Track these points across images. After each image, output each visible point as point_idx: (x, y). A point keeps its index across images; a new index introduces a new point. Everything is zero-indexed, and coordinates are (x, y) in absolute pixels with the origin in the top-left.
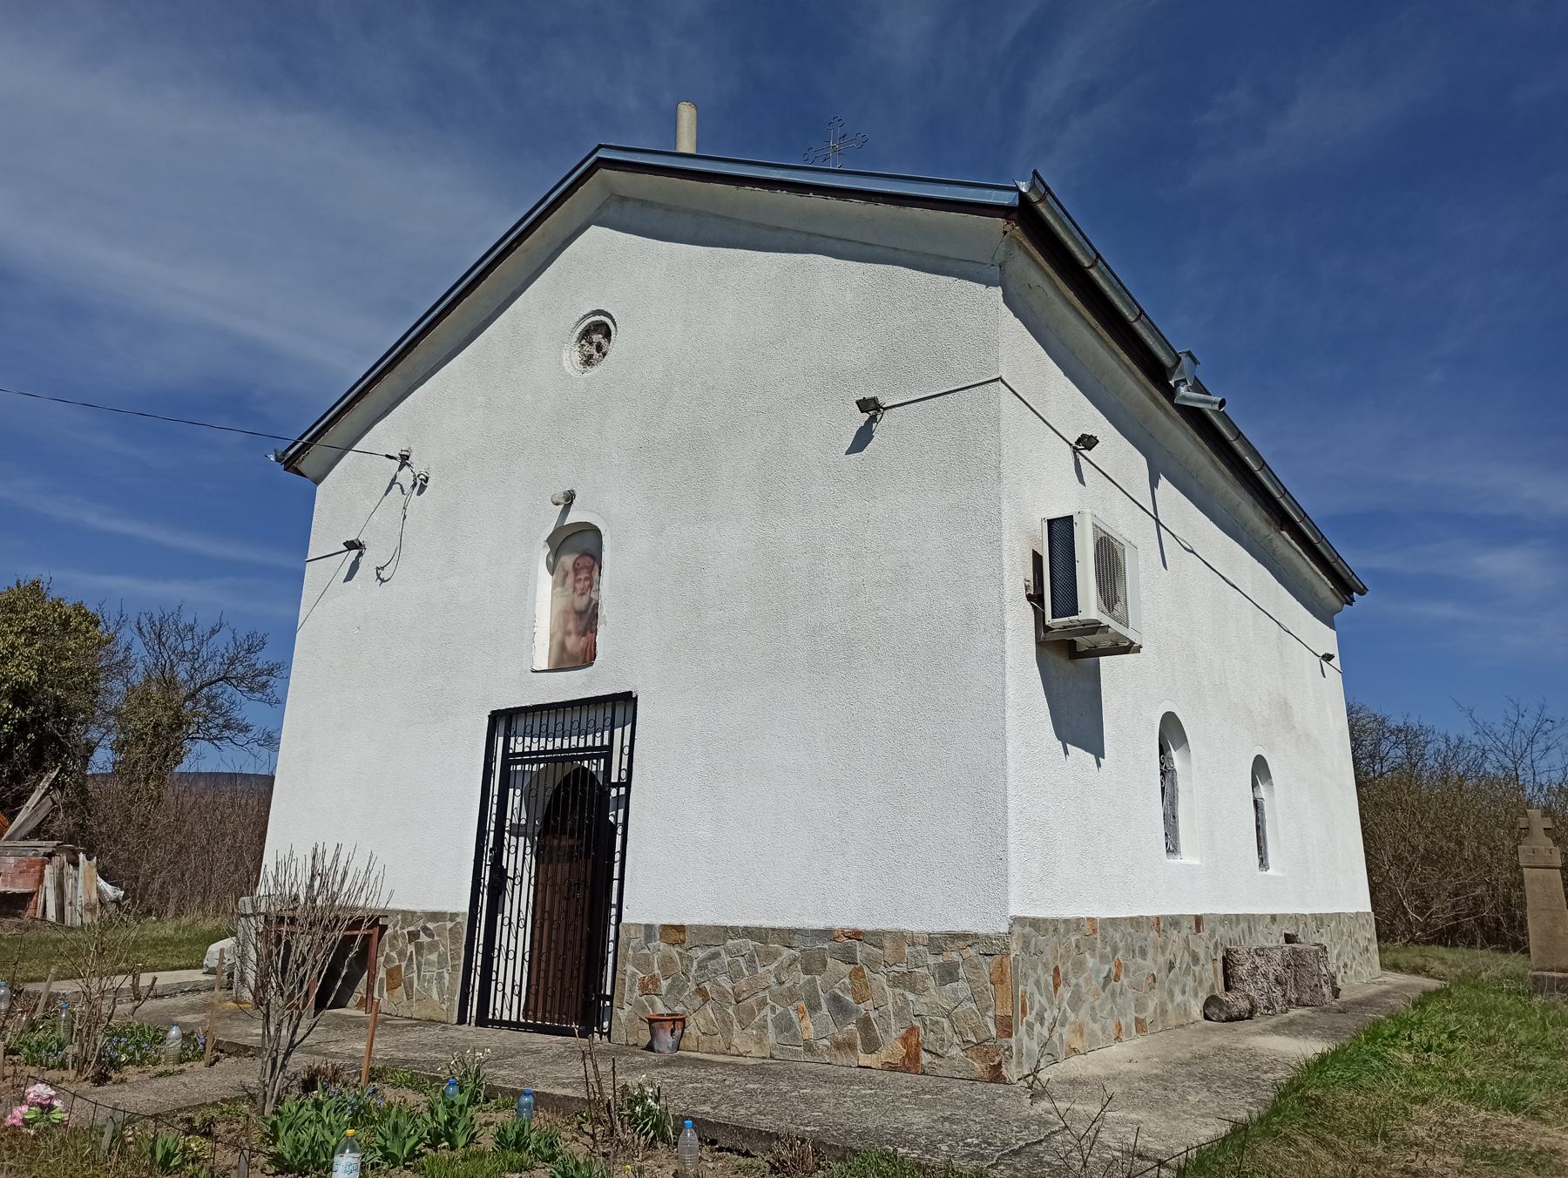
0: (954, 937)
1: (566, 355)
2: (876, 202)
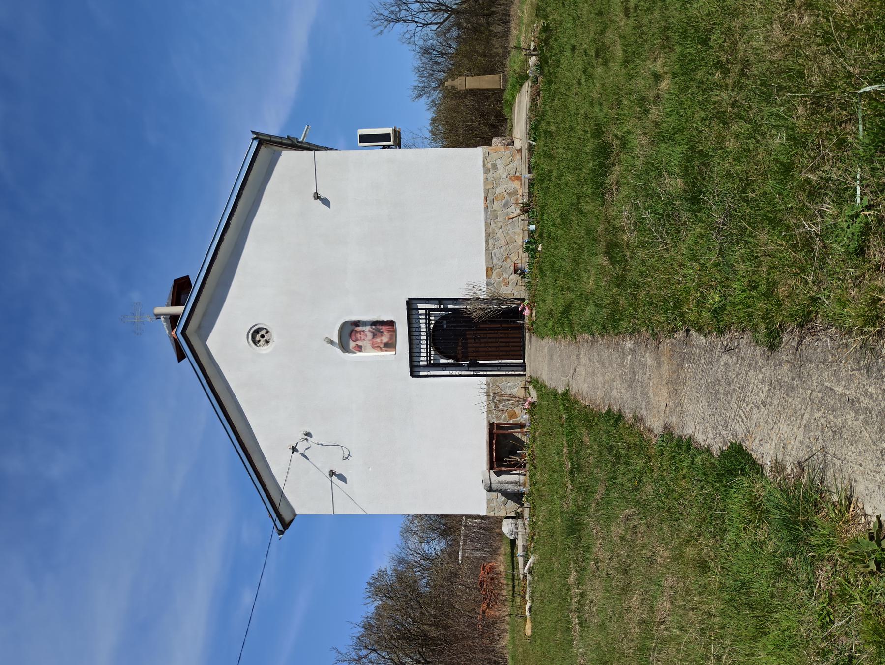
0: (484, 165)
1: (264, 352)
2: (233, 215)
